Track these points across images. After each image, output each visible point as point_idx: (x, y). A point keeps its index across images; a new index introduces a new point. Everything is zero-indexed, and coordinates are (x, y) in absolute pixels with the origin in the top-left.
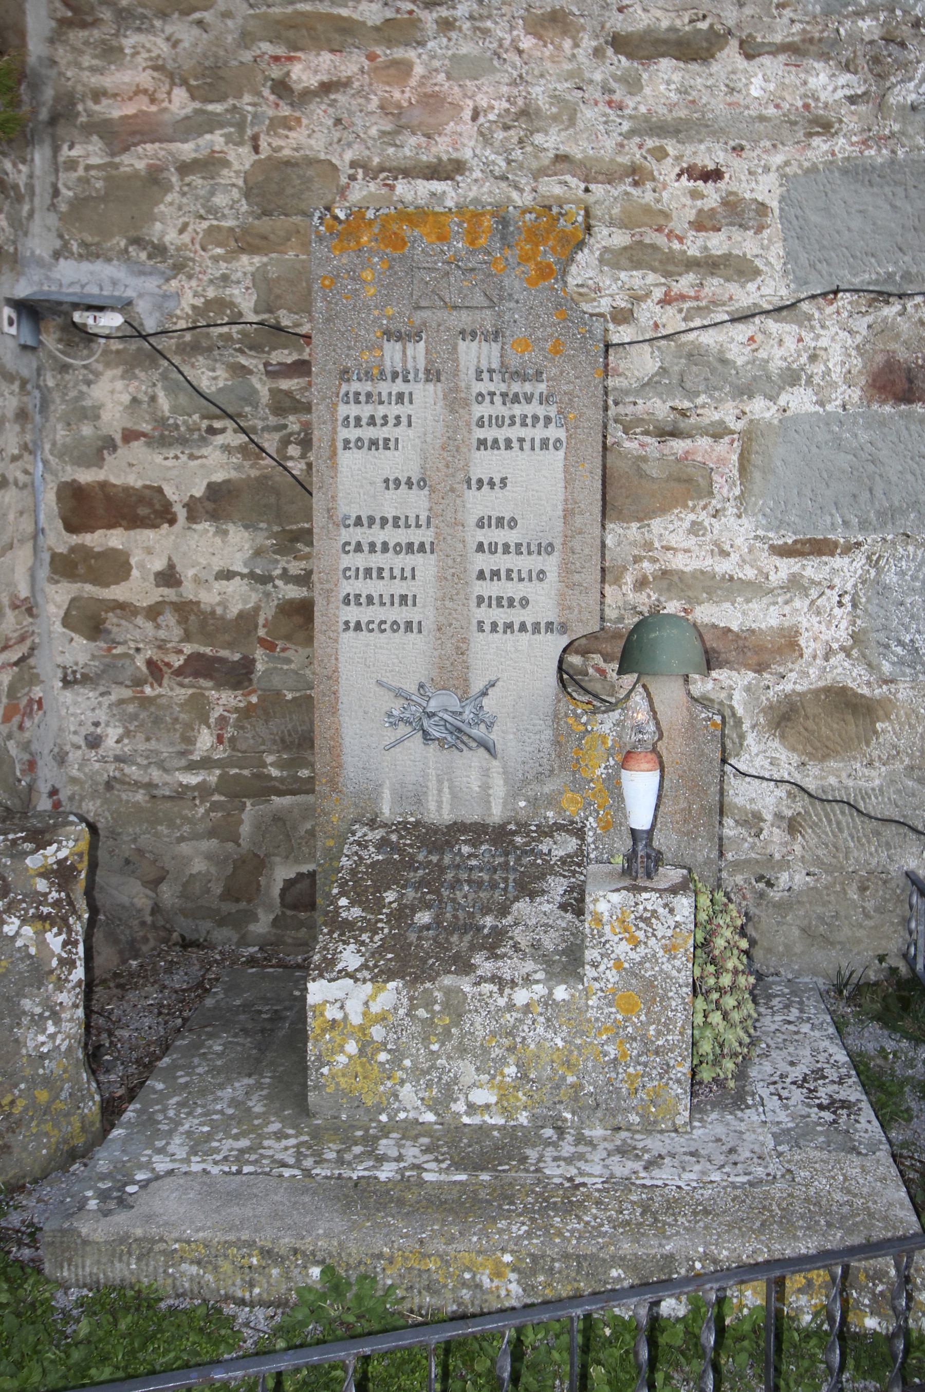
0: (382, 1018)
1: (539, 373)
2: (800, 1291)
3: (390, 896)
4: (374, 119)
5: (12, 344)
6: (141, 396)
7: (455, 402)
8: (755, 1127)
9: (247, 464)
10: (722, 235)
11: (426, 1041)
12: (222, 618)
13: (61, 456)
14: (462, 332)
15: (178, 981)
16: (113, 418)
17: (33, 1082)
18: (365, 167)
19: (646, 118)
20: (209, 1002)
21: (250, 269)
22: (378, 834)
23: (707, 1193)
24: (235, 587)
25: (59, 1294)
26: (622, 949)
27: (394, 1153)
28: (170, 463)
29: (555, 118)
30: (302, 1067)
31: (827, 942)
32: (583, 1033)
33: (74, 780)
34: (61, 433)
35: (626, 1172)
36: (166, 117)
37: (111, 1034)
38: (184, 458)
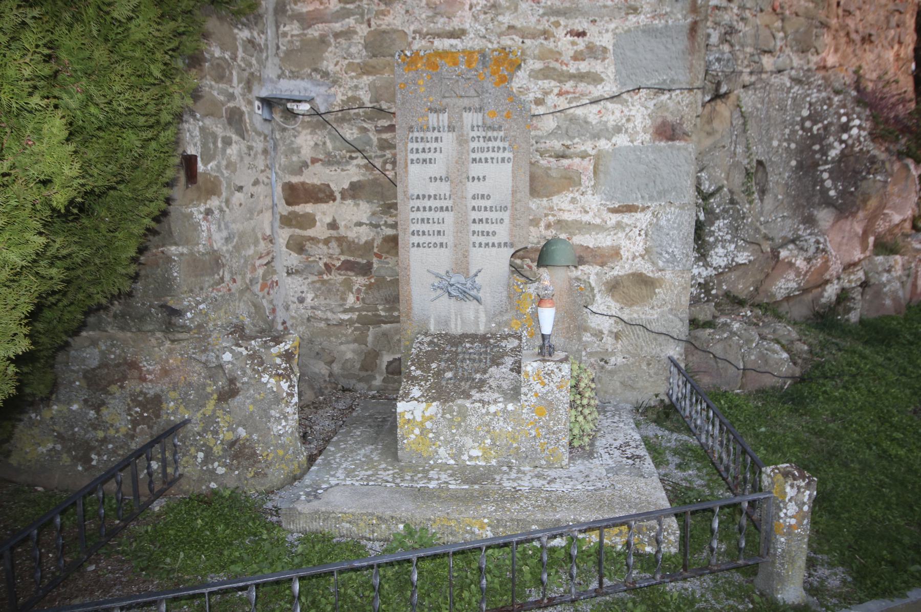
0: (430, 418)
1: (500, 127)
2: (617, 535)
3: (434, 365)
4: (424, 10)
5: (260, 118)
6: (319, 142)
7: (462, 141)
8: (598, 466)
9: (368, 173)
10: (586, 63)
11: (450, 428)
12: (358, 244)
13: (283, 171)
14: (465, 108)
15: (341, 405)
16: (307, 153)
17: (277, 446)
18: (420, 33)
19: (551, 8)
20: (354, 414)
21: (368, 82)
22: (428, 339)
23: (576, 494)
24: (363, 230)
25: (289, 536)
26: (538, 387)
27: (436, 477)
28: (333, 173)
29: (508, 8)
30: (395, 441)
31: (632, 388)
32: (520, 425)
33: (293, 317)
34: (283, 160)
35: (539, 485)
36: (328, 11)
37: (311, 428)
38: (339, 171)
